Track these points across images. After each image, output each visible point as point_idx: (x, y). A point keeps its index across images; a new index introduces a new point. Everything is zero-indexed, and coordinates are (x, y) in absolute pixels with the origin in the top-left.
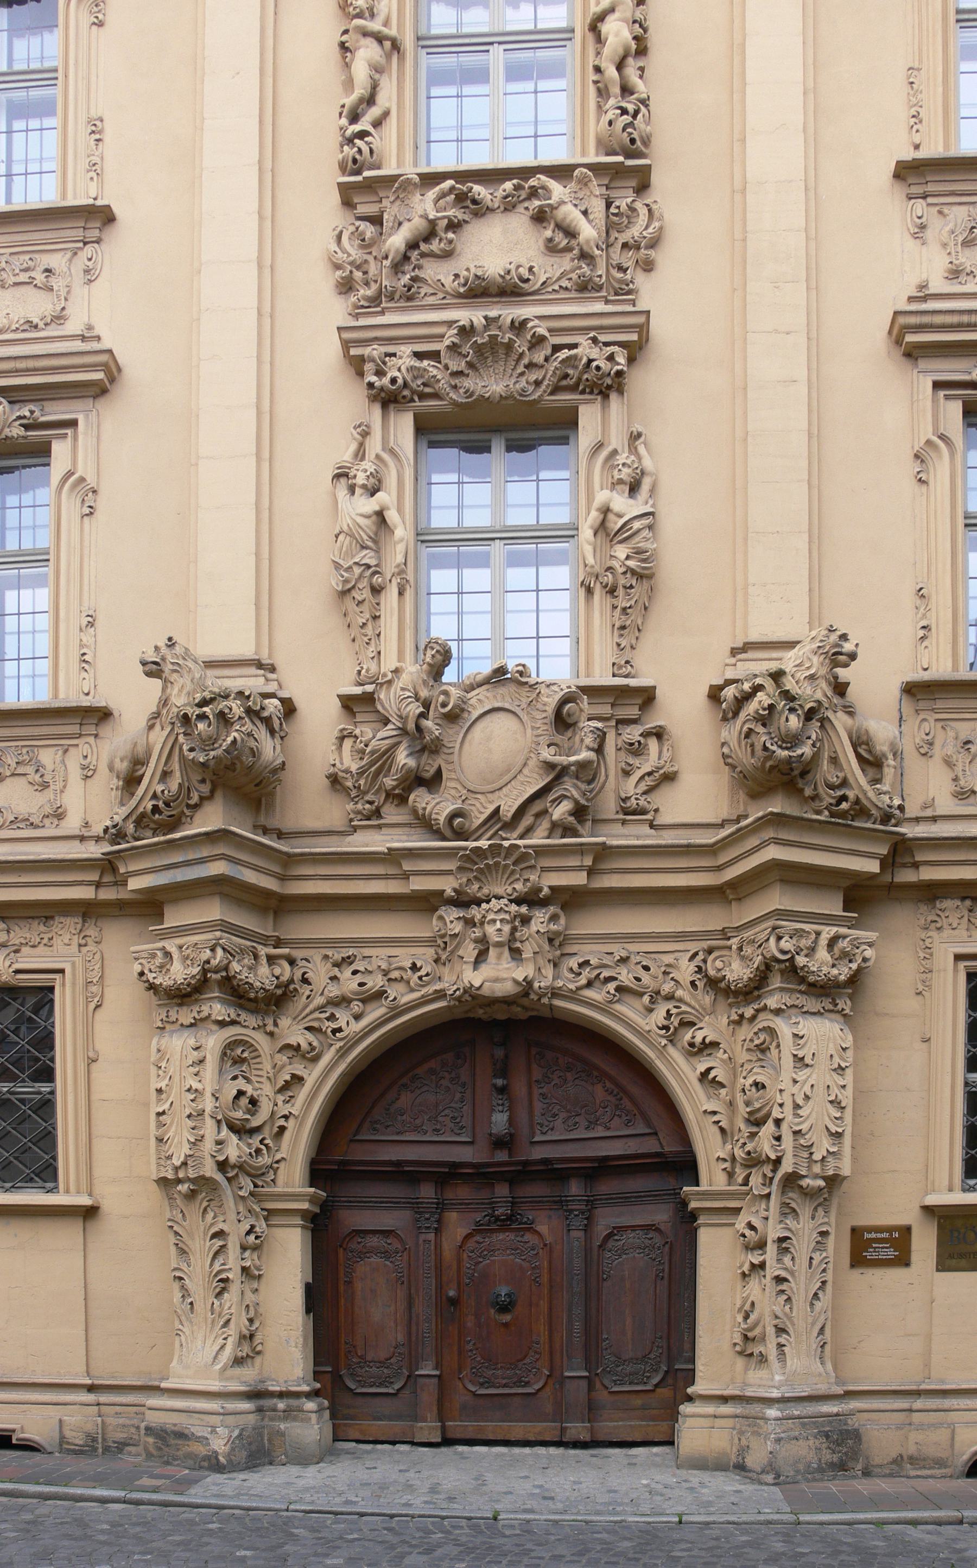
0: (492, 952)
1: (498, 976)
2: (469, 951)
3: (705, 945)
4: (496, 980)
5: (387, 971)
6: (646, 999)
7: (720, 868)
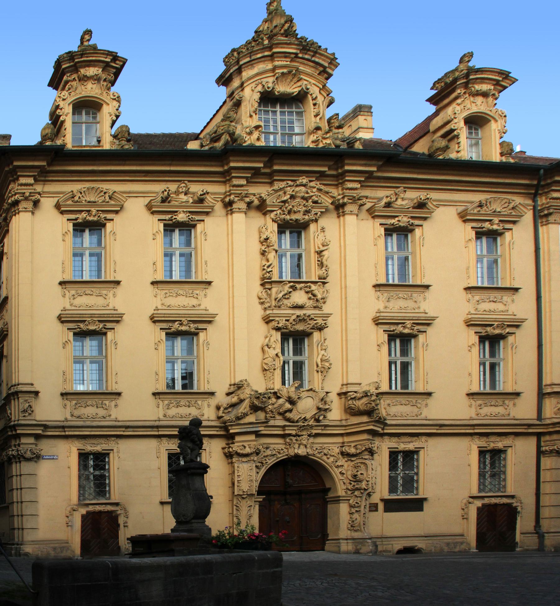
0: (302, 446)
1: (302, 451)
2: (297, 446)
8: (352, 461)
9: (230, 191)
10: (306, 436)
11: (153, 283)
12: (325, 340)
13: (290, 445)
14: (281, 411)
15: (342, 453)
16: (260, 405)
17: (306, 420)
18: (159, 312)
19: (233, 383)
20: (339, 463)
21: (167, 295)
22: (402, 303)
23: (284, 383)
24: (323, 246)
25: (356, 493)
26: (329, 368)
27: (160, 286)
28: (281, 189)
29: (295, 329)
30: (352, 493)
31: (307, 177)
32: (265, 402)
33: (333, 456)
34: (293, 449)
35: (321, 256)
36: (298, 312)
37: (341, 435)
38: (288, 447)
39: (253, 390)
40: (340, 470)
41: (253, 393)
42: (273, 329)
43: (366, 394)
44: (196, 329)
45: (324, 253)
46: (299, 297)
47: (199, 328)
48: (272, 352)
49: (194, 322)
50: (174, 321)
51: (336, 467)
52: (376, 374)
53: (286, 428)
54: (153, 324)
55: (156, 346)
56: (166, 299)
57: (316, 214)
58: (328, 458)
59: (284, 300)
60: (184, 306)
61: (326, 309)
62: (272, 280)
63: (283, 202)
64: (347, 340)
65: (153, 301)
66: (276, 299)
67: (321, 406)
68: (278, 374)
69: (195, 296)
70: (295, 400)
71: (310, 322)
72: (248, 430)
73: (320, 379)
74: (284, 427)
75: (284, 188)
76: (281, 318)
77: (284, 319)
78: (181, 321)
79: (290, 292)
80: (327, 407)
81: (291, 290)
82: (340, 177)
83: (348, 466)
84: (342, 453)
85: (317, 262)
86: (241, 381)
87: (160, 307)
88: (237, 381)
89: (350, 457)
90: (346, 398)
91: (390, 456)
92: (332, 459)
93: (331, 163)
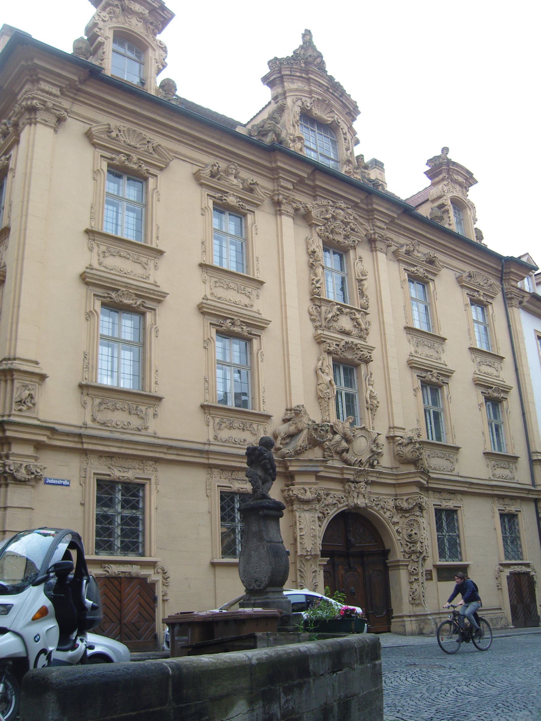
0: (360, 496)
1: (361, 502)
2: (355, 495)
3: (394, 497)
7: (396, 479)
8: (406, 517)
9: (278, 190)
10: (363, 484)
11: (201, 265)
12: (371, 374)
13: (349, 492)
14: (338, 449)
15: (399, 509)
16: (318, 439)
18: (209, 302)
19: (289, 407)
20: (395, 520)
21: (218, 285)
23: (338, 417)
24: (362, 275)
25: (414, 557)
26: (377, 407)
30: (409, 557)
32: (323, 436)
33: (389, 510)
35: (361, 285)
37: (394, 485)
38: (347, 495)
39: (310, 420)
41: (310, 423)
43: (411, 441)
45: (364, 282)
46: (345, 323)
47: (253, 333)
49: (248, 325)
52: (416, 422)
53: (345, 471)
54: (201, 316)
57: (354, 241)
58: (385, 513)
59: (333, 322)
62: (321, 297)
63: (326, 219)
66: (326, 319)
67: (375, 449)
69: (247, 294)
71: (359, 352)
72: (309, 469)
74: (343, 468)
75: (326, 205)
76: (332, 342)
77: (335, 343)
78: (233, 319)
79: (338, 315)
80: (380, 451)
81: (339, 313)
82: (370, 213)
83: (403, 523)
84: (396, 507)
85: (358, 290)
86: (298, 406)
87: (209, 297)
88: (294, 405)
89: (404, 513)
90: (394, 443)
92: (388, 513)
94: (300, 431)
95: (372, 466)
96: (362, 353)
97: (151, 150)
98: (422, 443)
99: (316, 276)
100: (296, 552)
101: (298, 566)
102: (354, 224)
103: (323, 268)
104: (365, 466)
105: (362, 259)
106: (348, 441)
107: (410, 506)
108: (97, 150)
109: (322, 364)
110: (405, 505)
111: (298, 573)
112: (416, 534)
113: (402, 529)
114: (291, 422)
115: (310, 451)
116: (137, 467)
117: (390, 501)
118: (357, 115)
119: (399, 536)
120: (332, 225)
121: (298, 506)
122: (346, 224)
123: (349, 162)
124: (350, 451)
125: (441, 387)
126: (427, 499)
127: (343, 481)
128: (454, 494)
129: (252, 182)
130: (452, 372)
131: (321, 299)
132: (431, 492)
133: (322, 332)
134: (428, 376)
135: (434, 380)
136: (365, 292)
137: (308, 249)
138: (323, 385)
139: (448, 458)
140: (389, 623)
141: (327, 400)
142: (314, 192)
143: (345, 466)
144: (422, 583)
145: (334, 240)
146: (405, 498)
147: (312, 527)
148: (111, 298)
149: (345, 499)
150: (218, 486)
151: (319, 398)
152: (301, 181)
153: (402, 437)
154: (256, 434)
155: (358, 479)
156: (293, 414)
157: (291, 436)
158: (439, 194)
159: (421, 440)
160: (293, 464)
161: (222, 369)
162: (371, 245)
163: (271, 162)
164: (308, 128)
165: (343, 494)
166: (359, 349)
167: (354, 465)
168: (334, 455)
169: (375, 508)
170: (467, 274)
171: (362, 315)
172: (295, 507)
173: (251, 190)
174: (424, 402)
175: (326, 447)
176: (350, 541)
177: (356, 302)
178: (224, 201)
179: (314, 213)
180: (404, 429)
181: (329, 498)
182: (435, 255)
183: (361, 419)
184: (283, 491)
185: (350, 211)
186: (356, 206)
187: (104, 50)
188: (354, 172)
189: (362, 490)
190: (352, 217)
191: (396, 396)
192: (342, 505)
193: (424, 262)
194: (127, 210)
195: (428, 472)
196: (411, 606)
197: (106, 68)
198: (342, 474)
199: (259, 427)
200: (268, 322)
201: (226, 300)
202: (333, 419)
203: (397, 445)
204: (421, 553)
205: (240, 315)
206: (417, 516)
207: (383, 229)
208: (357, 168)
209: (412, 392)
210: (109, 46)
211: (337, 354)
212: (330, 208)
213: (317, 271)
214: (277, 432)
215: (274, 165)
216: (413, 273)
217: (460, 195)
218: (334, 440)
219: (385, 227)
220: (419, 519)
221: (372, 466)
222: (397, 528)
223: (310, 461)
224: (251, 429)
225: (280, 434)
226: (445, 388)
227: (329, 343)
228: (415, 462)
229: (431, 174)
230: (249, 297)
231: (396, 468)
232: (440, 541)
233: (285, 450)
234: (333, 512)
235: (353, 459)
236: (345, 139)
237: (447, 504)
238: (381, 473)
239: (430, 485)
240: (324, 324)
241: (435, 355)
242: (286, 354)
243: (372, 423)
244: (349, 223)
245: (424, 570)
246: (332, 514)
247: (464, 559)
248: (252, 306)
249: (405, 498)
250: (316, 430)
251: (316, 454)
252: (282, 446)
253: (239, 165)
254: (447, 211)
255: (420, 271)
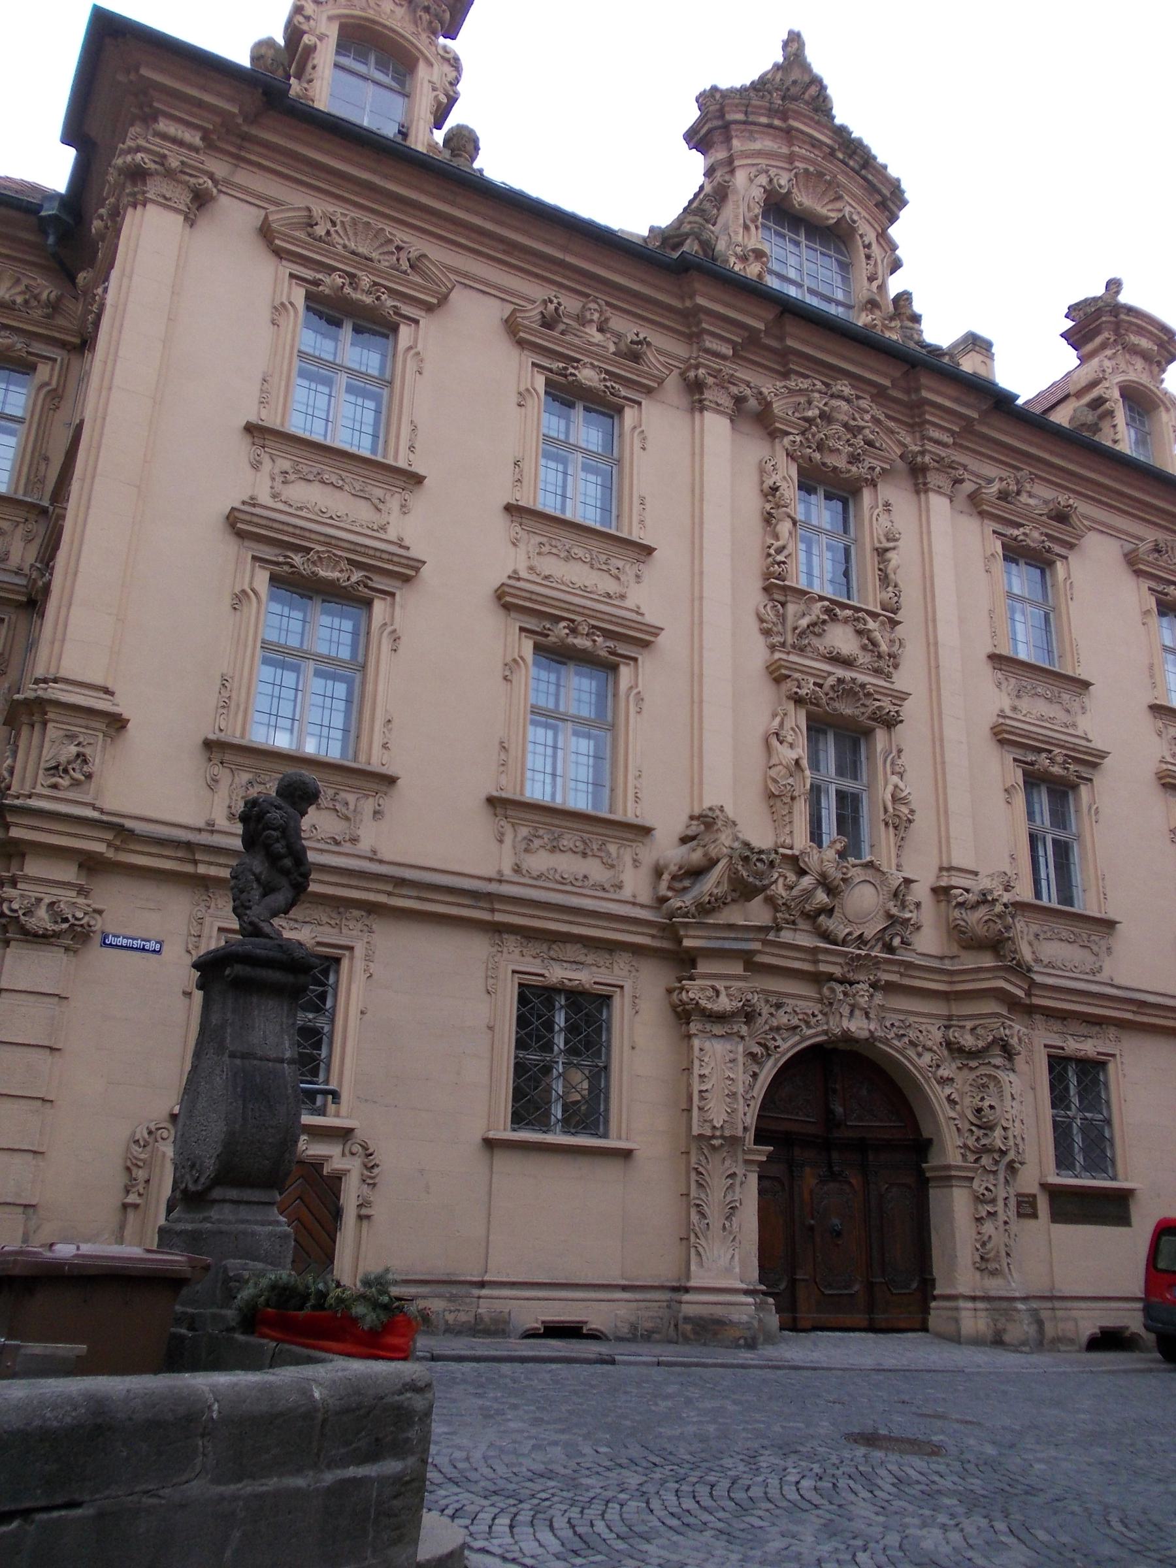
0: (857, 1012)
1: (858, 1026)
2: (846, 1010)
3: (946, 1023)
4: (861, 1029)
5: (801, 1018)
6: (920, 1049)
7: (951, 983)
8: (971, 1069)
9: (696, 358)
10: (866, 986)
11: (509, 509)
12: (900, 751)
13: (831, 1004)
14: (808, 907)
17: (866, 943)
19: (697, 812)
20: (944, 1072)
21: (545, 549)
22: (1042, 708)
24: (888, 540)
25: (986, 1161)
26: (910, 821)
27: (529, 522)
28: (800, 390)
29: (835, 710)
30: (977, 1161)
31: (853, 387)
34: (838, 1016)
36: (841, 672)
38: (826, 1010)
40: (948, 1091)
42: (789, 698)
44: (610, 653)
45: (889, 555)
46: (841, 639)
48: (787, 754)
49: (608, 634)
50: (558, 619)
51: (938, 1083)
52: (1008, 860)
53: (821, 957)
55: (507, 673)
56: (541, 559)
57: (873, 469)
58: (919, 1055)
59: (811, 636)
60: (584, 589)
61: (902, 680)
63: (806, 419)
64: (943, 763)
65: (504, 556)
68: (801, 810)
70: (836, 883)
71: (868, 702)
73: (892, 844)
74: (815, 950)
75: (806, 390)
76: (805, 677)
77: (812, 680)
78: (573, 621)
79: (824, 622)
81: (826, 617)
84: (949, 1045)
85: (877, 572)
87: (523, 574)
91: (1051, 1069)
93: (898, 374)
94: (713, 863)
95: (889, 948)
96: (878, 704)
97: (405, 265)
98: (1020, 907)
99: (777, 538)
100: (690, 1127)
101: (693, 1159)
102: (872, 432)
103: (795, 523)
104: (872, 948)
105: (891, 509)
106: (831, 891)
107: (981, 1044)
108: (284, 263)
109: (782, 724)
110: (968, 1041)
111: (693, 1176)
112: (991, 1107)
113: (962, 1095)
114: (695, 843)
115: (735, 907)
116: (325, 919)
117: (934, 1029)
118: (900, 209)
119: (954, 1109)
120: (821, 432)
121: (700, 1026)
122: (855, 431)
123: (872, 305)
124: (835, 914)
125: (1075, 787)
126: (1024, 1030)
127: (818, 979)
128: (1100, 1024)
129: (635, 338)
130: (1103, 755)
131: (785, 589)
132: (1037, 1017)
133: (784, 656)
134: (1043, 760)
135: (1056, 770)
136: (892, 576)
137: (762, 482)
138: (780, 767)
139: (1086, 944)
140: (926, 1310)
141: (789, 800)
142: (783, 364)
143: (822, 945)
144: (1006, 1223)
145: (824, 464)
146: (969, 1024)
147: (728, 1073)
148: (292, 566)
149: (820, 1017)
150: (514, 972)
151: (771, 796)
152: (752, 339)
153: (967, 891)
154: (612, 866)
155: (851, 976)
156: (702, 827)
157: (696, 873)
158: (1092, 376)
159: (1018, 899)
160: (692, 933)
161: (547, 726)
162: (916, 478)
163: (682, 299)
164: (778, 234)
165: (816, 1008)
166: (868, 695)
167: (844, 943)
168: (799, 921)
169: (896, 1042)
170: (1150, 546)
171: (883, 623)
172: (694, 1028)
173: (636, 357)
174: (1031, 815)
175: (780, 902)
176: (832, 1112)
177: (871, 598)
178: (571, 378)
179: (778, 407)
180: (976, 874)
181: (781, 1012)
182: (1071, 502)
183: (872, 846)
184: (670, 991)
185: (864, 403)
186: (880, 394)
187: (315, 62)
188: (884, 325)
189: (863, 1001)
190: (867, 417)
191: (959, 800)
192: (813, 1031)
193: (1044, 518)
194: (347, 391)
195: (1029, 970)
196: (978, 1274)
197: (317, 97)
198: (816, 962)
199: (622, 850)
200: (656, 631)
201: (563, 583)
202: (800, 841)
203: (955, 907)
204: (1003, 1153)
205: (591, 613)
206: (998, 1067)
207: (945, 445)
208: (892, 319)
209: (1002, 796)
210: (325, 56)
211: (817, 705)
212: (816, 395)
213: (779, 528)
214: (662, 862)
215: (688, 304)
216: (1015, 539)
217: (1145, 379)
218: (799, 888)
219: (951, 441)
220: (1000, 1074)
221: (889, 948)
222: (948, 1091)
223: (731, 927)
224: (603, 854)
225: (666, 867)
226: (1084, 790)
227: (798, 680)
228: (996, 945)
229: (1076, 338)
230: (619, 579)
231: (952, 958)
232: (1061, 1132)
233: (676, 903)
234: (788, 1047)
235: (842, 931)
236: (868, 257)
237: (1078, 1046)
238: (910, 965)
239: (1036, 1001)
240: (790, 641)
241: (1061, 716)
242: (696, 703)
243: (898, 856)
244: (862, 428)
245: (1012, 1192)
246: (788, 1050)
247: (1120, 1177)
248: (623, 597)
249: (969, 1024)
250: (746, 859)
251: (756, 913)
252: (670, 894)
253: (608, 304)
254: (1110, 413)
255: (1033, 536)
